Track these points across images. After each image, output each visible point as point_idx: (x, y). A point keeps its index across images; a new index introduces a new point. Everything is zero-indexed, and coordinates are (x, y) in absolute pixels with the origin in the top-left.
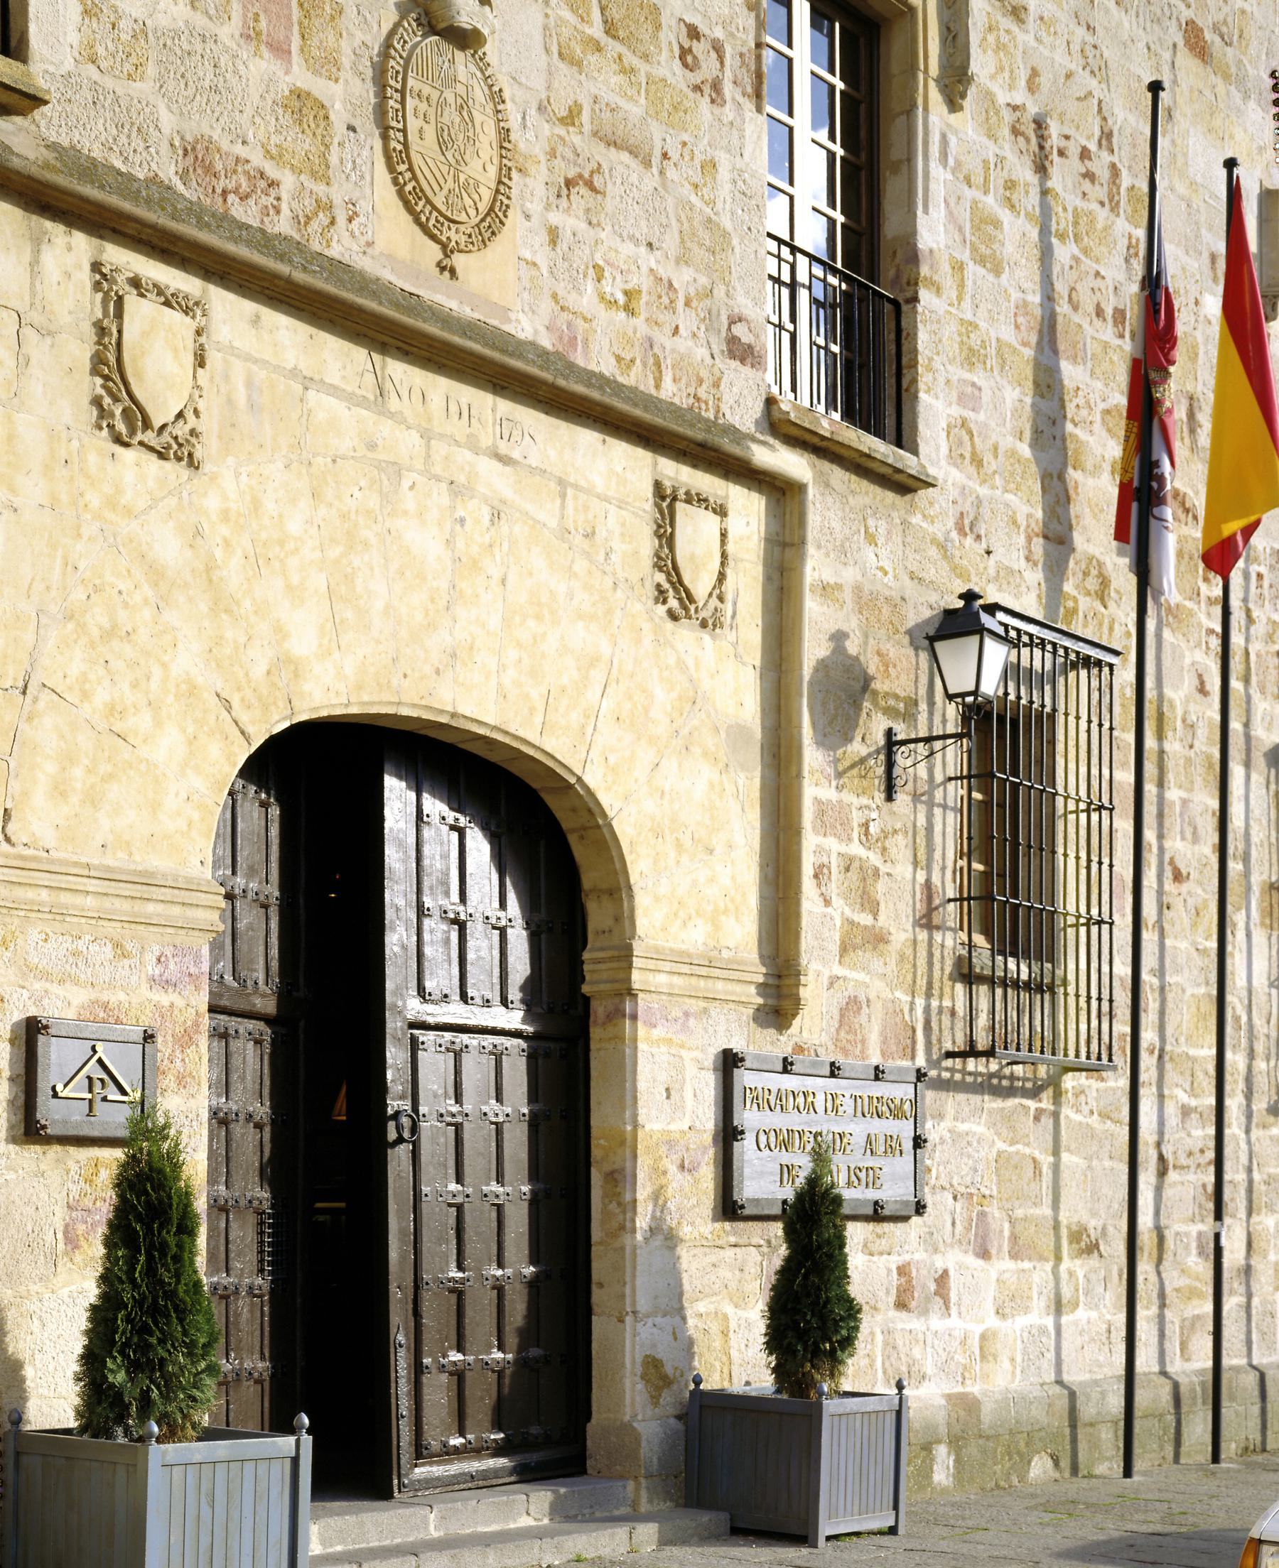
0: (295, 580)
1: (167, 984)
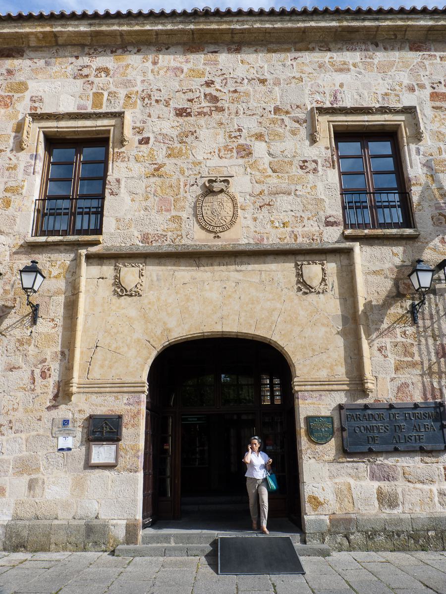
0: (170, 312)
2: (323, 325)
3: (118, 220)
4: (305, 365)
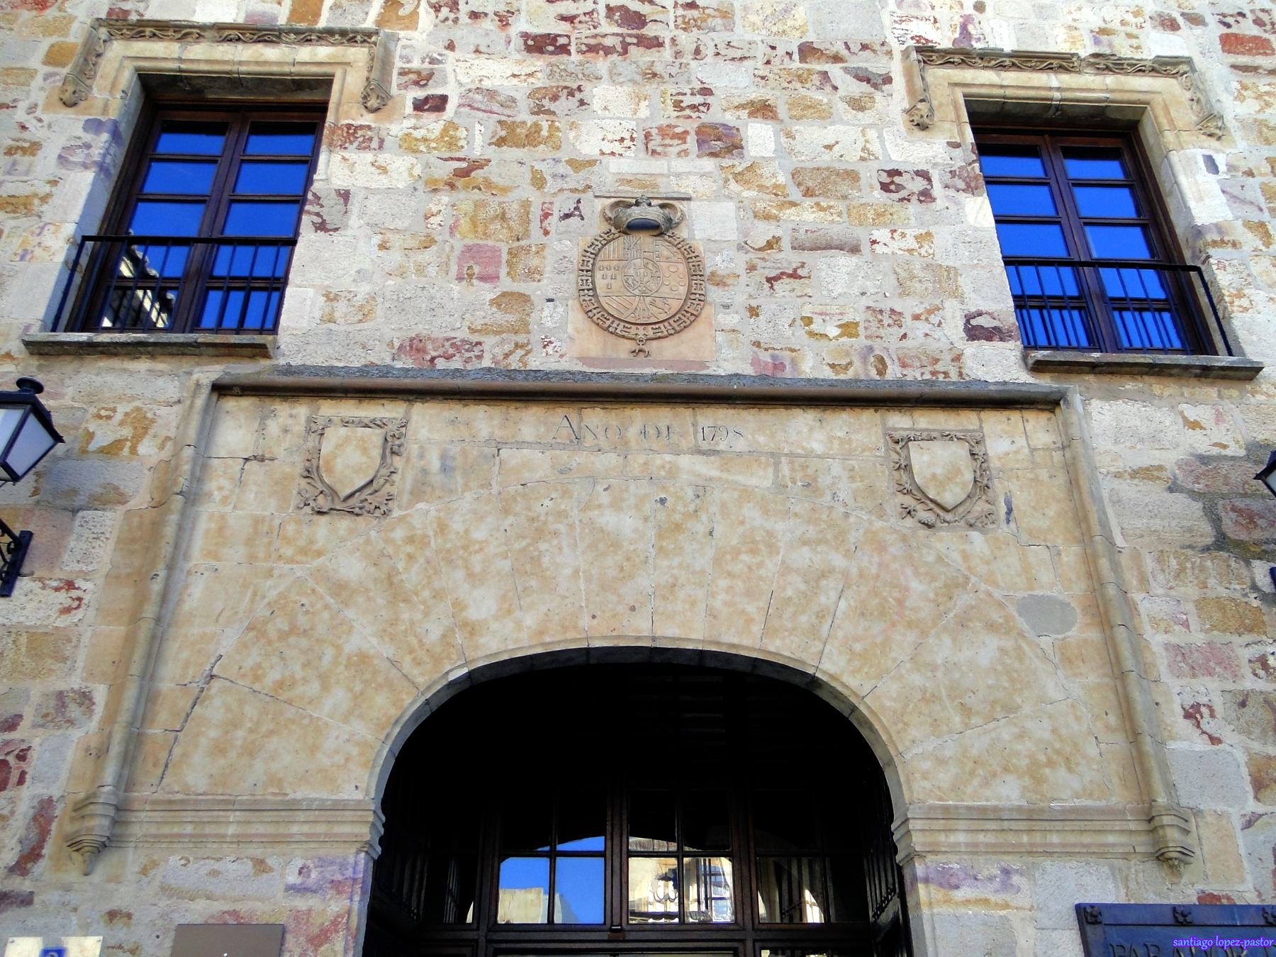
0: (477, 569)
2: (991, 627)
3: (331, 298)
4: (941, 762)
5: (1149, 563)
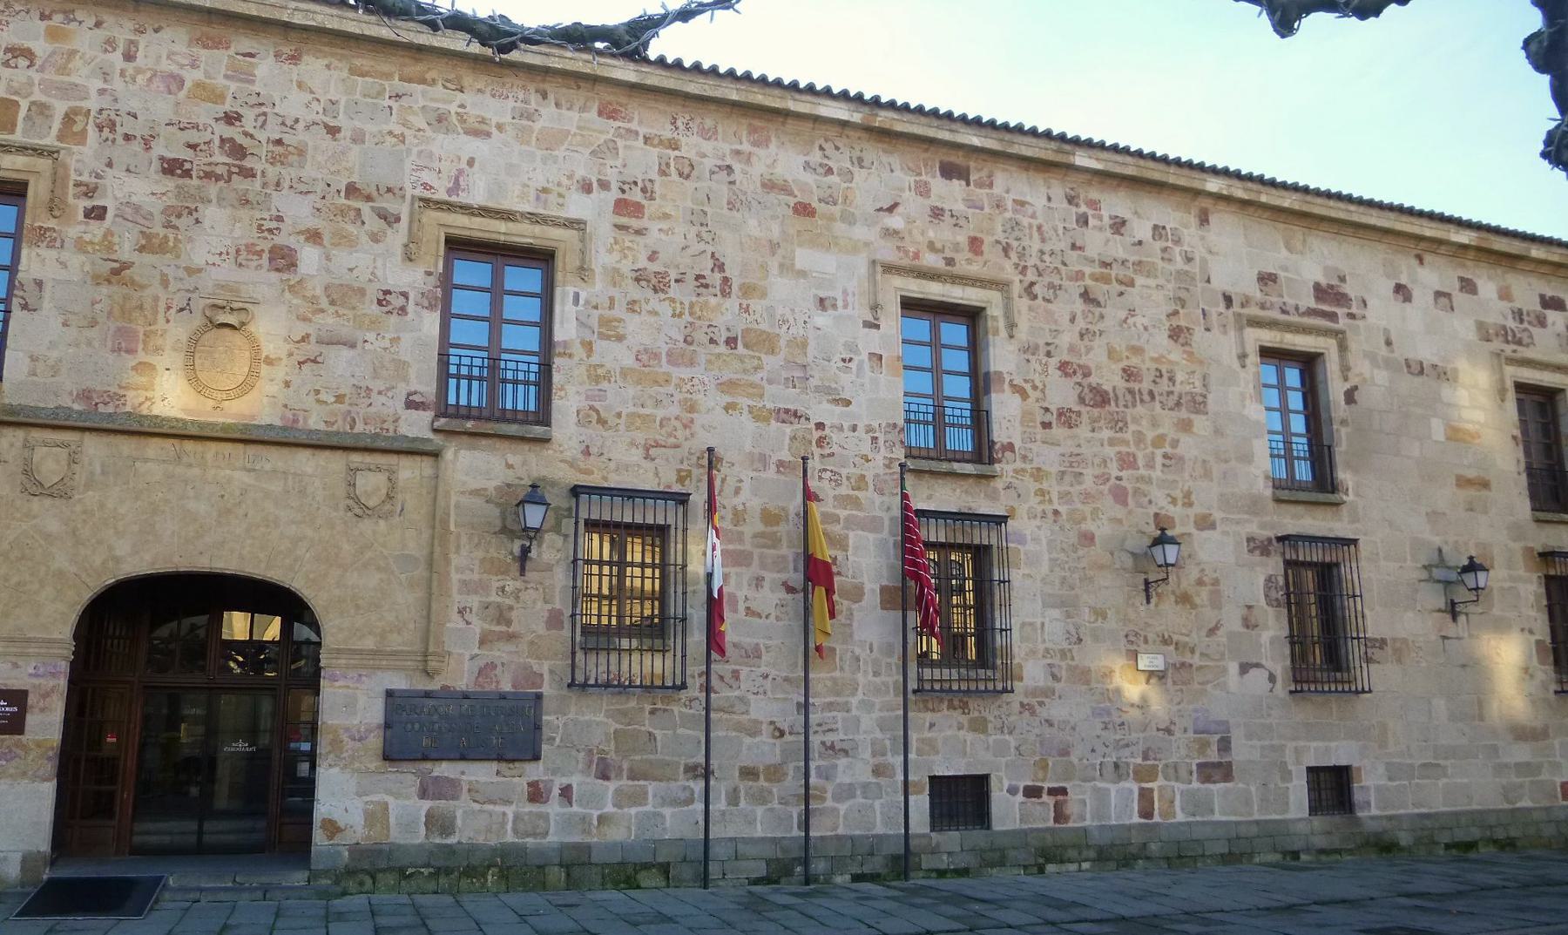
1: (36, 676)
2: (378, 569)
3: (34, 359)
5: (464, 539)
